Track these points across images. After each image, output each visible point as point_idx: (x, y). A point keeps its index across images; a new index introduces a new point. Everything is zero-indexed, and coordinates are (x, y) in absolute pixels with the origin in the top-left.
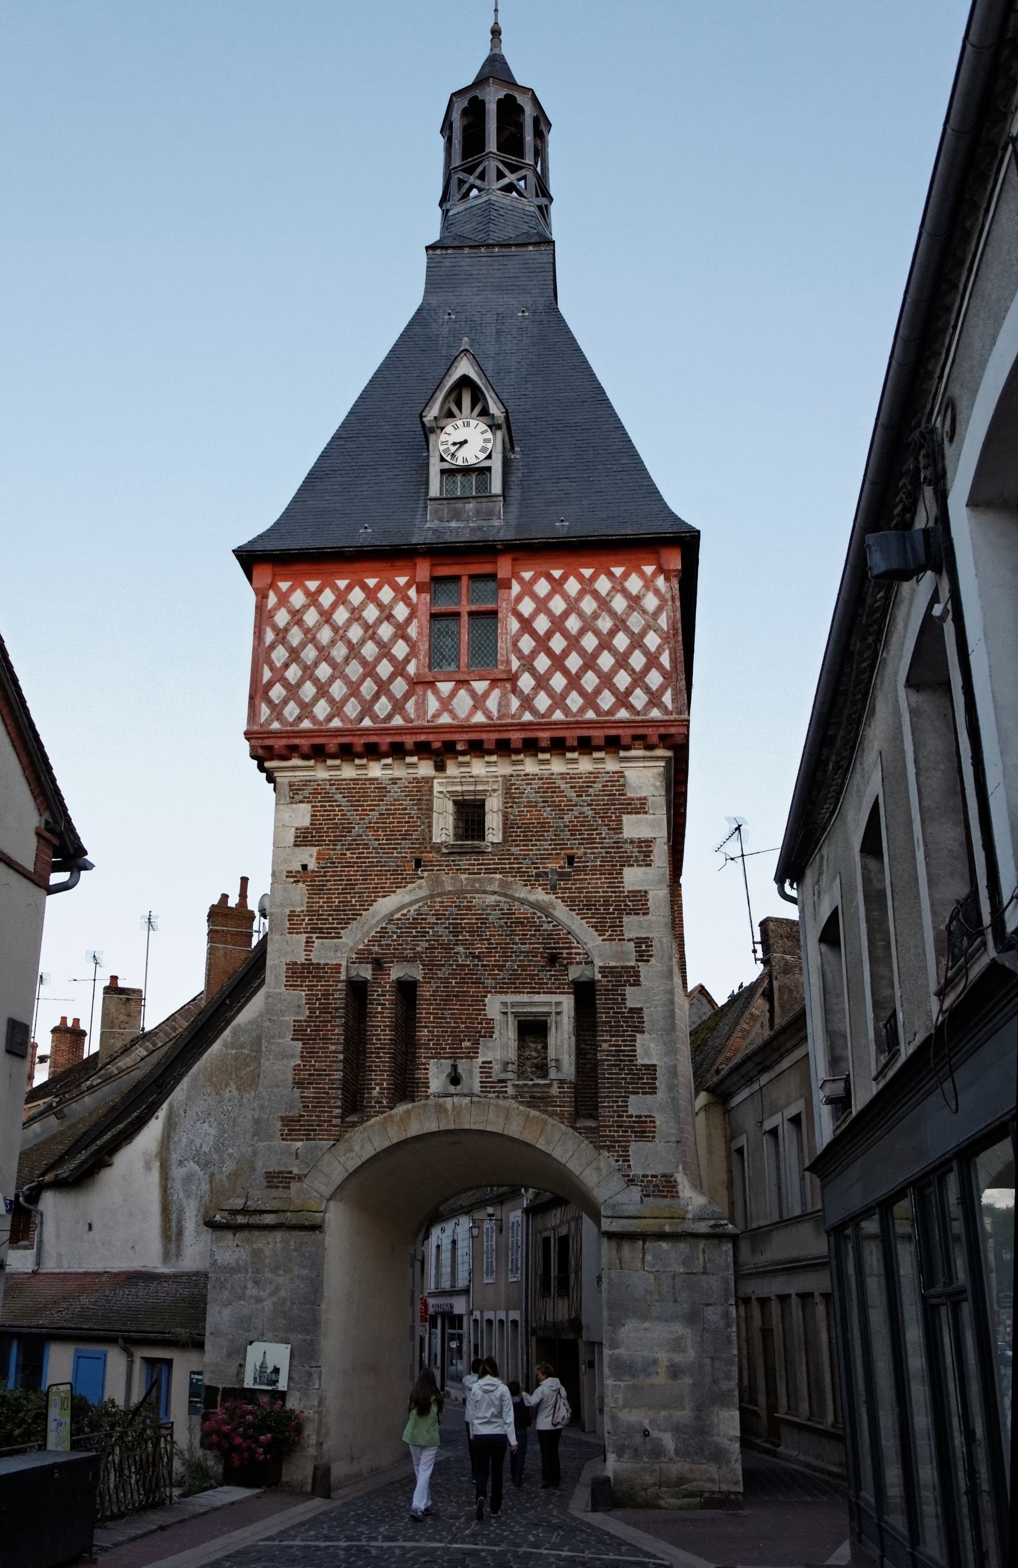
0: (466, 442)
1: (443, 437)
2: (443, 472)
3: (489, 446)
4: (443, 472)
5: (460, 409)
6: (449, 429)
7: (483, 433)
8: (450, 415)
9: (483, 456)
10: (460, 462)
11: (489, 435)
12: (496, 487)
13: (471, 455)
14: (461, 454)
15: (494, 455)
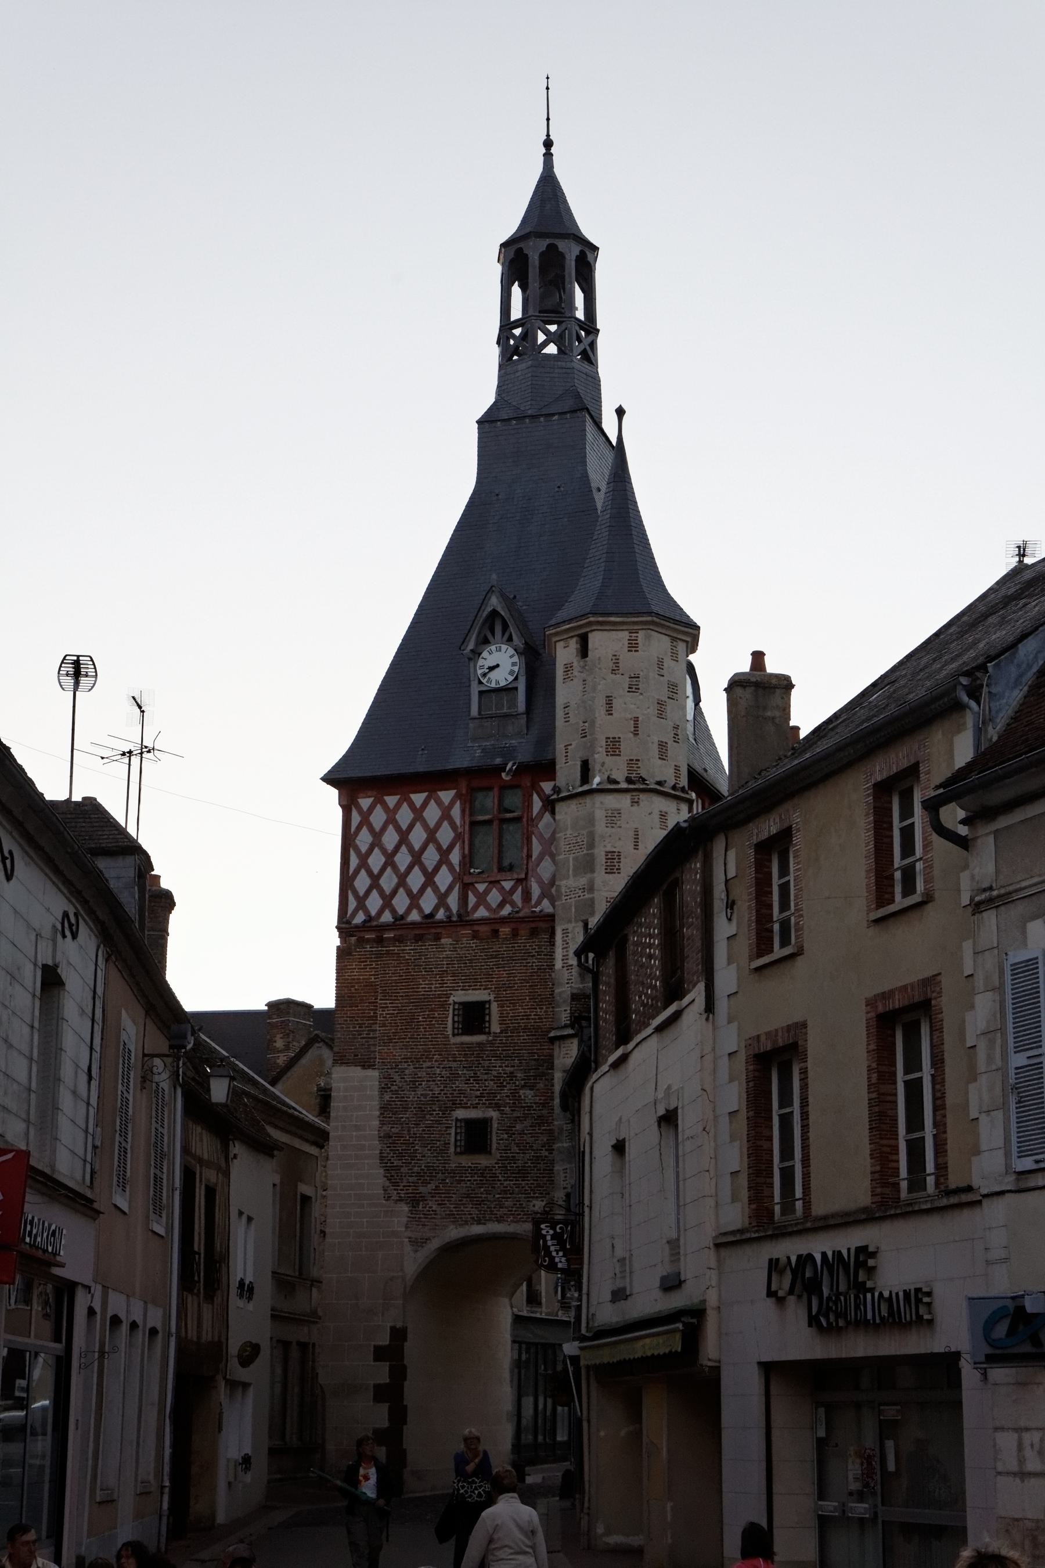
0: (498, 666)
1: (481, 662)
2: (481, 693)
3: (516, 669)
4: (481, 693)
5: (493, 635)
6: (485, 654)
7: (511, 657)
8: (486, 642)
9: (511, 678)
10: (493, 685)
11: (516, 659)
12: (521, 706)
13: (501, 678)
14: (494, 675)
15: (520, 677)
